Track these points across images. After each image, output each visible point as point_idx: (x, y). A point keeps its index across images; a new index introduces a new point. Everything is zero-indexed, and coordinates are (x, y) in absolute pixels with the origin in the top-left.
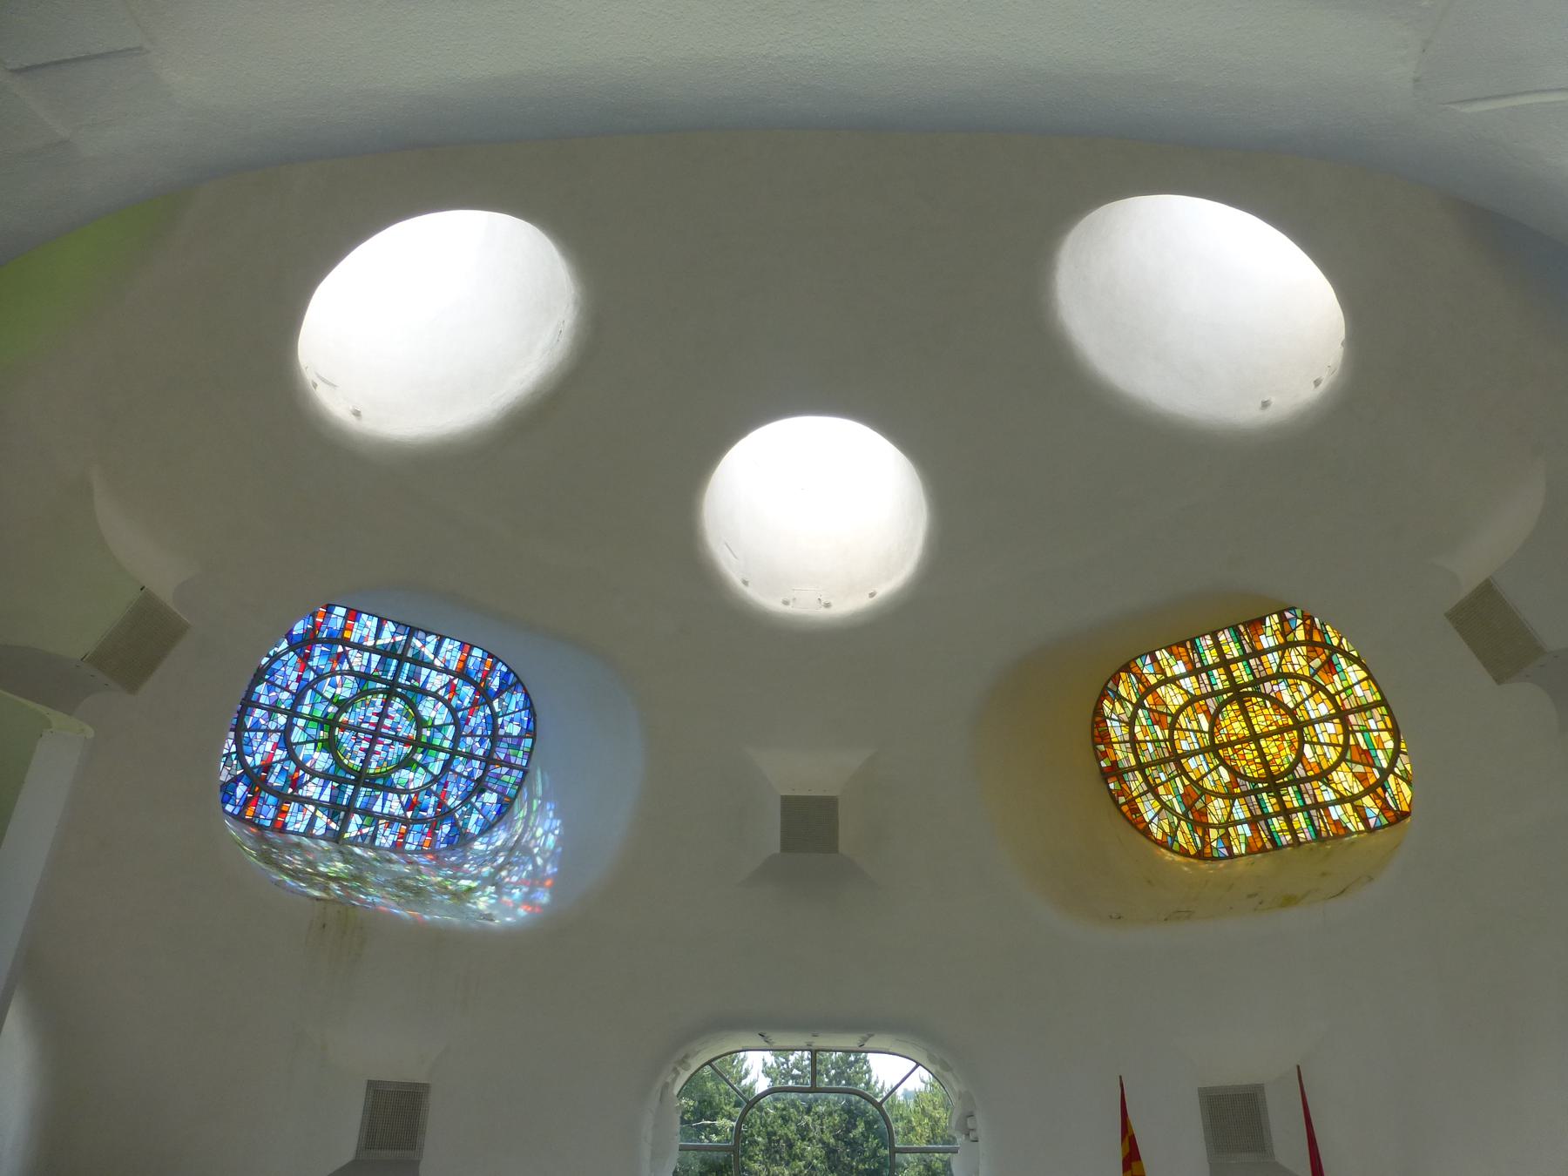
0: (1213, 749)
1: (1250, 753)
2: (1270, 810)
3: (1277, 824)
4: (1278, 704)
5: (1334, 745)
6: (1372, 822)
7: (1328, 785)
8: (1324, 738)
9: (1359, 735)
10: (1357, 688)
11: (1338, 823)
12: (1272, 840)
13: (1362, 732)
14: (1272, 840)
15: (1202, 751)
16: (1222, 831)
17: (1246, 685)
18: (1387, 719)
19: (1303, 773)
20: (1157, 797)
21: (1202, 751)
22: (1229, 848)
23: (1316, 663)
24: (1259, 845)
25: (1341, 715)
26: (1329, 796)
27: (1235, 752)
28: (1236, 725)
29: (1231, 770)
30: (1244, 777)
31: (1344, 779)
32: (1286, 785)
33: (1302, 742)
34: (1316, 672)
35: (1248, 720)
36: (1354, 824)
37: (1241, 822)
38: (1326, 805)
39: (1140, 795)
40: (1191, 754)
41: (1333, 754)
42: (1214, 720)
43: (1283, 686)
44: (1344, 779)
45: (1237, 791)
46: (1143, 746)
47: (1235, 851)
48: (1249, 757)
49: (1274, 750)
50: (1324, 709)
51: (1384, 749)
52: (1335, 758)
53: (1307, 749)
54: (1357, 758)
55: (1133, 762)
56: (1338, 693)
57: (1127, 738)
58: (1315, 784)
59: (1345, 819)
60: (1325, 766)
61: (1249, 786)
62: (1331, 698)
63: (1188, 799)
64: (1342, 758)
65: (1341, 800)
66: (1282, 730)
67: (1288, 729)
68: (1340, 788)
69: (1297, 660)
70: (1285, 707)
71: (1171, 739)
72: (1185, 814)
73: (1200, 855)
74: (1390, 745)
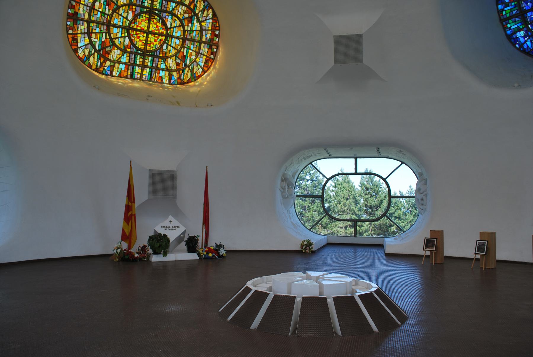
0: (128, 29)
1: (143, 37)
2: (138, 63)
3: (137, 69)
4: (164, 24)
5: (175, 49)
6: (172, 81)
7: (165, 62)
8: (173, 45)
9: (186, 49)
10: (195, 32)
11: (160, 77)
12: (132, 75)
13: (187, 49)
14: (132, 75)
15: (122, 27)
16: (112, 64)
17: (156, 10)
18: (198, 48)
19: (158, 54)
20: (90, 38)
21: (122, 27)
22: (111, 72)
23: (187, 16)
24: (125, 75)
25: (184, 39)
26: (163, 66)
27: (137, 34)
28: (143, 23)
29: (131, 40)
30: (135, 46)
31: (171, 63)
32: (149, 55)
33: (164, 42)
34: (185, 19)
35: (149, 24)
36: (166, 80)
37: (123, 63)
38: (160, 69)
39: (81, 33)
40: (116, 26)
41: (173, 52)
42: (135, 17)
43: (170, 17)
44: (171, 63)
45: (128, 50)
46: (96, 12)
47: (114, 74)
48: (141, 38)
49: (153, 41)
50: (179, 34)
51: (190, 58)
52: (173, 53)
53: (165, 46)
54: (180, 57)
55: (86, 17)
56: (188, 31)
57: (90, 5)
58: (160, 60)
59: (164, 77)
60: (167, 55)
61: (134, 50)
62: (184, 31)
63: (103, 45)
64: (175, 55)
65: (167, 70)
66: (160, 34)
67: (162, 35)
68: (168, 65)
69: (181, 11)
70: (166, 26)
71: (111, 16)
72: (99, 51)
73: (97, 70)
74: (193, 57)
